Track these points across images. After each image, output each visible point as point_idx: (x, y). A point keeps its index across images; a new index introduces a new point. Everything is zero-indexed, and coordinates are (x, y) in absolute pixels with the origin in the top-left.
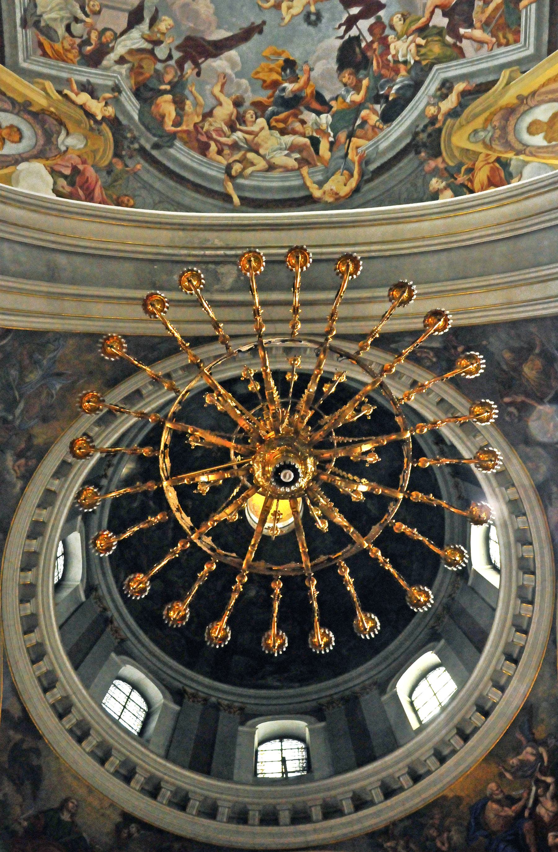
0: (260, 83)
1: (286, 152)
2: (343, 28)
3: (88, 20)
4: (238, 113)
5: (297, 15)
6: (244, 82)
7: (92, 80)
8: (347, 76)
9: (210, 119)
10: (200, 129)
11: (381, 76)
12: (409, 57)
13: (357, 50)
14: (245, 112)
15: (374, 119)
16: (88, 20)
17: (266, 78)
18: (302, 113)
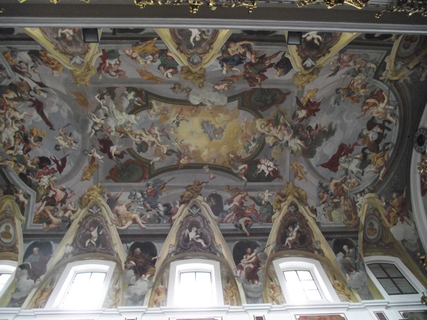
0: (32, 129)
1: (7, 138)
2: (54, 159)
3: (29, 68)
4: (19, 121)
5: (58, 142)
6: (31, 123)
7: (7, 69)
8: (37, 160)
9: (13, 111)
10: (8, 107)
11: (36, 172)
12: (41, 183)
13: (46, 164)
14: (20, 123)
15: (21, 170)
16: (29, 68)
17: (34, 130)
18: (23, 143)
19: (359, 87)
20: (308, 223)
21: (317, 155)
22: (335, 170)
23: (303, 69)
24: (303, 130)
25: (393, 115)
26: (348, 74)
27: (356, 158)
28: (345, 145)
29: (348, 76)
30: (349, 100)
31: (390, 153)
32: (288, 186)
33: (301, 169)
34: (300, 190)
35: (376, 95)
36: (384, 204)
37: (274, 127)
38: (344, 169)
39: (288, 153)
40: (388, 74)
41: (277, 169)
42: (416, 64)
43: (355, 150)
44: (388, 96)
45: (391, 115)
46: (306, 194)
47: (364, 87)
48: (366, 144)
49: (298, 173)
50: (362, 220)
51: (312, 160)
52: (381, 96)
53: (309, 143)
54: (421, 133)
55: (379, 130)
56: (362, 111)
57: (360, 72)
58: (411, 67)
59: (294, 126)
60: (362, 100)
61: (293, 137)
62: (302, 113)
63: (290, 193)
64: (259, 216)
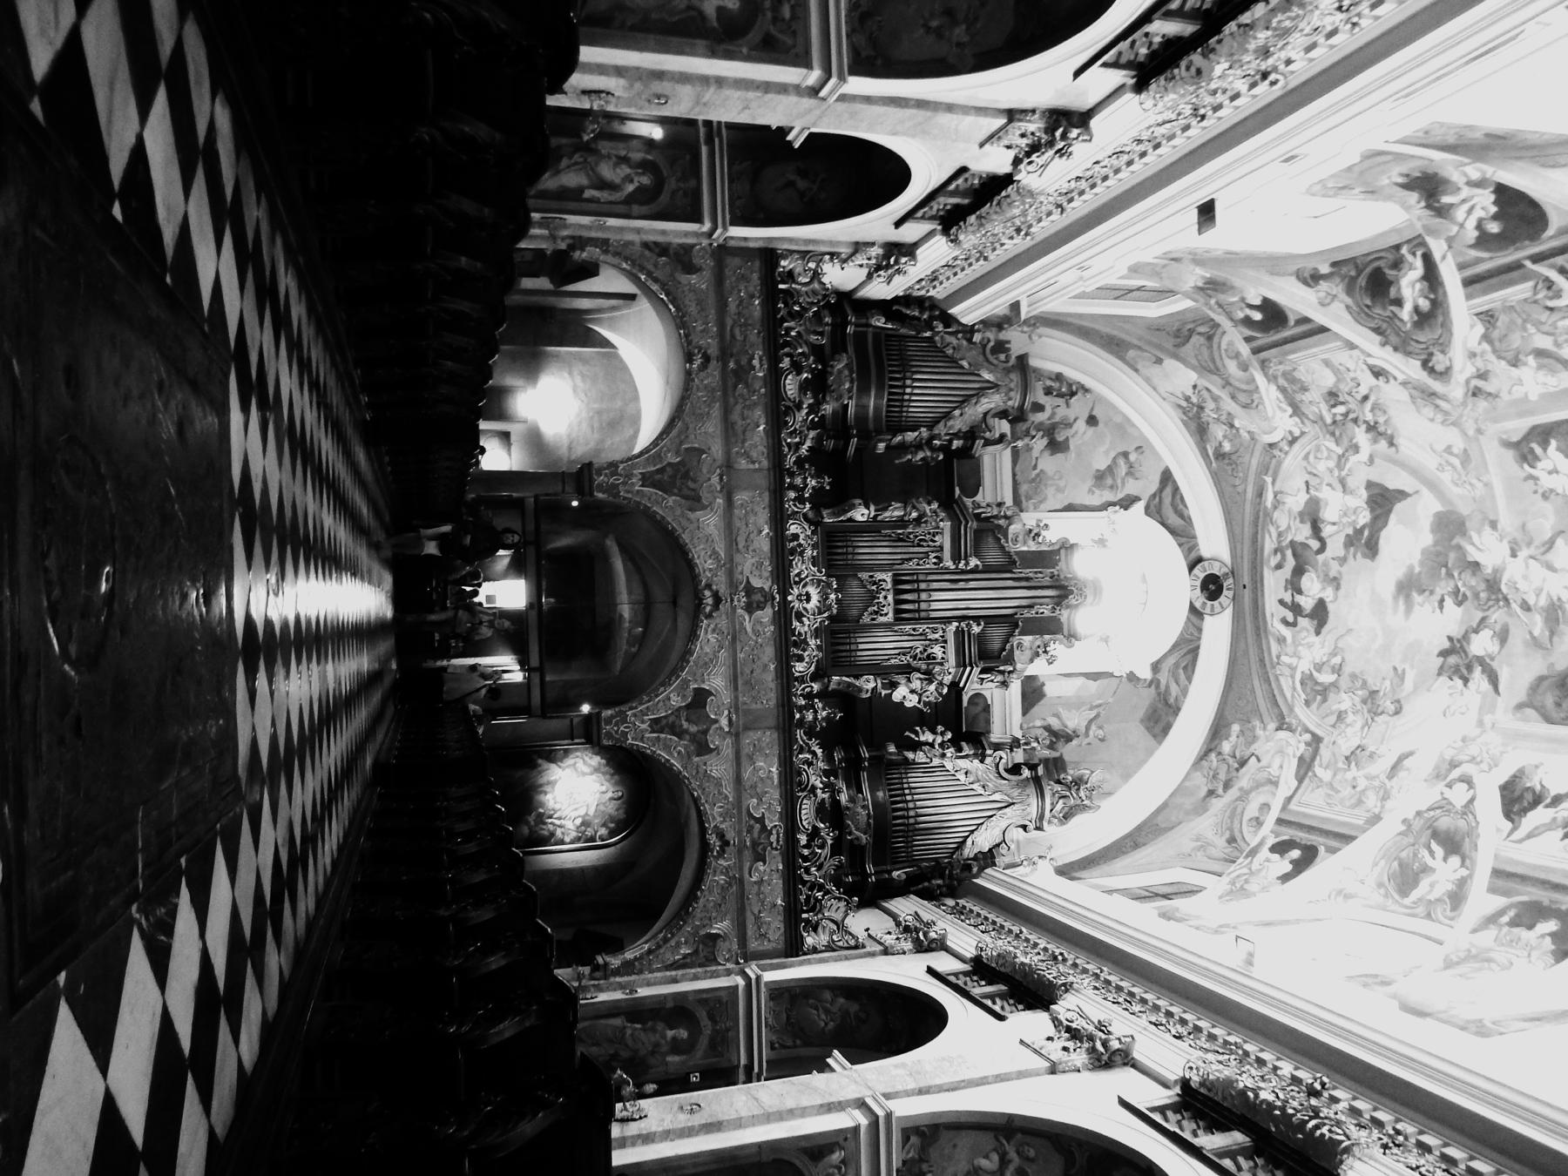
19: (1350, 718)
20: (1378, 338)
21: (1426, 523)
22: (1370, 485)
23: (1475, 780)
24: (1476, 596)
25: (1281, 640)
26: (1372, 755)
27: (1334, 524)
28: (1365, 556)
29: (1372, 749)
30: (1374, 684)
31: (1269, 545)
32: (1476, 421)
33: (1456, 477)
34: (1439, 417)
35: (1318, 692)
36: (1237, 424)
37: (1559, 599)
38: (1351, 493)
39: (1506, 522)
40: (1296, 745)
41: (1526, 466)
42: (1244, 769)
43: (1342, 546)
44: (1294, 689)
45: (1284, 639)
46: (1419, 412)
47: (1341, 716)
48: (1320, 562)
49: (1463, 467)
50: (1260, 379)
51: (1438, 507)
52: (1308, 690)
53: (1452, 556)
54: (1216, 603)
55: (1300, 599)
56: (1342, 650)
57: (1347, 758)
58: (1253, 759)
59: (1501, 603)
60: (1344, 682)
61: (1498, 572)
62: (1481, 644)
63: (1464, 404)
64: (1525, 321)
